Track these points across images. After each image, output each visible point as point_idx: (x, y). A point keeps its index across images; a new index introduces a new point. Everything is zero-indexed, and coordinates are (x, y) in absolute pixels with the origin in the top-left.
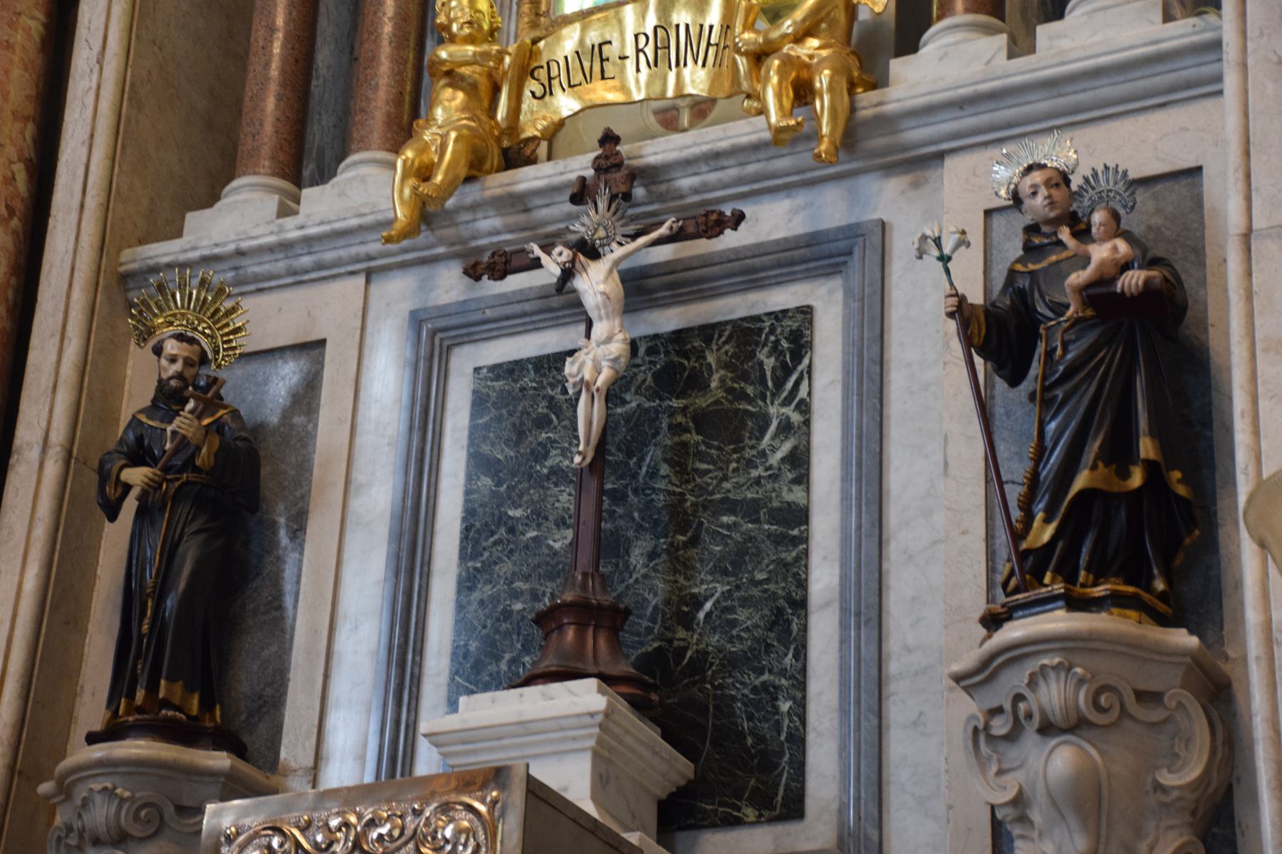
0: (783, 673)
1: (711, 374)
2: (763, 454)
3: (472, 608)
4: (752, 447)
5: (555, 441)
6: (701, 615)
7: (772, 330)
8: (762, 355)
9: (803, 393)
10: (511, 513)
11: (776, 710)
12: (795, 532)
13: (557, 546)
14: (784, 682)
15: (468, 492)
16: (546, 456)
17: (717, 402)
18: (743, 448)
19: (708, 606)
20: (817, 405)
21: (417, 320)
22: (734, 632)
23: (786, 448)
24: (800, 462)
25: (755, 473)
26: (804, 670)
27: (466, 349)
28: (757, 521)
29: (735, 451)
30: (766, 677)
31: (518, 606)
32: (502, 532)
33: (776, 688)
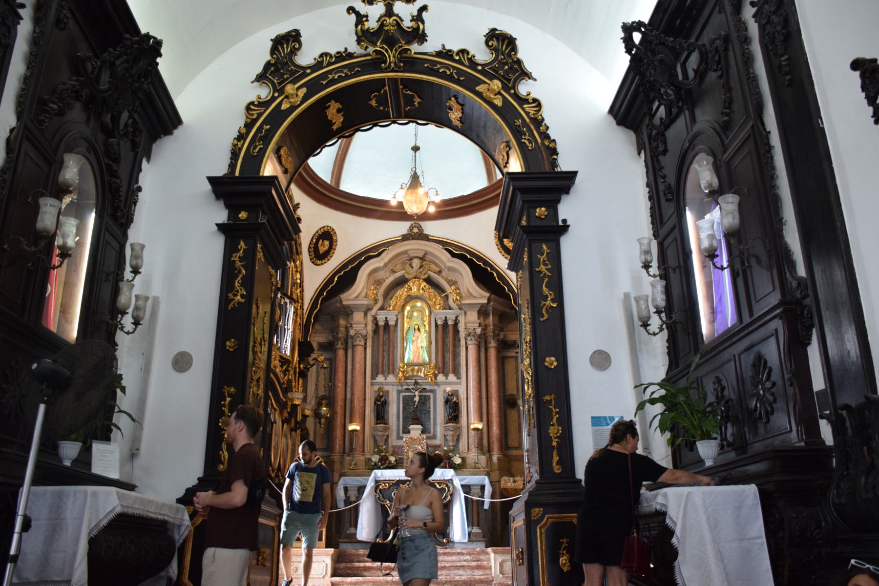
21: (398, 390)
24: (430, 407)
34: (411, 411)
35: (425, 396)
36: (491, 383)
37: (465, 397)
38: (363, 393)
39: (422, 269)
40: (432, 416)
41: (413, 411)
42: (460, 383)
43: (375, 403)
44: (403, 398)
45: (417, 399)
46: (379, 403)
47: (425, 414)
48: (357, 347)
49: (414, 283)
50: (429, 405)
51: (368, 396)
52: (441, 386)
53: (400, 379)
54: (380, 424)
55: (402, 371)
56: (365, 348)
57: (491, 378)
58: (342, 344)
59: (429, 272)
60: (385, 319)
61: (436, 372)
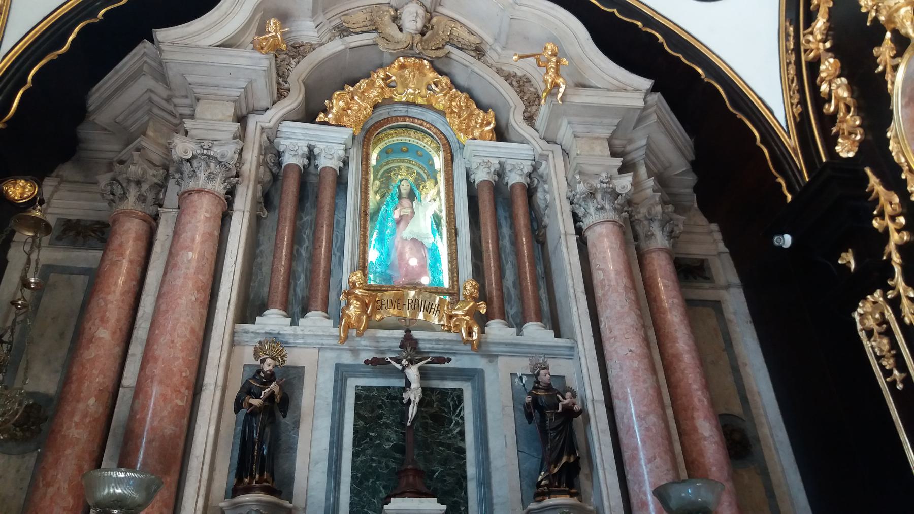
0: (461, 498)
1: (434, 403)
2: (451, 430)
3: (358, 463)
4: (448, 427)
5: (384, 414)
6: (435, 477)
7: (452, 394)
8: (449, 400)
9: (462, 414)
10: (370, 434)
11: (460, 510)
12: (462, 456)
13: (386, 447)
14: (461, 501)
15: (354, 425)
16: (382, 418)
17: (436, 412)
18: (444, 427)
19: (437, 474)
20: (465, 418)
21: (338, 367)
22: (445, 483)
23: (458, 429)
24: (462, 434)
25: (449, 435)
26: (467, 498)
27: (353, 379)
28: (450, 450)
29: (442, 428)
30: (456, 499)
31: (374, 465)
32: (368, 440)
33: (460, 502)
34: (388, 446)
35: (444, 392)
36: (677, 356)
37: (599, 395)
38: (194, 357)
39: (427, 34)
40: (471, 470)
41: (396, 448)
42: (571, 353)
43: (238, 406)
44: (358, 397)
45: (414, 395)
46: (256, 402)
47: (445, 462)
48: (195, 197)
49: (402, 67)
50: (460, 424)
51: (213, 376)
52: (501, 361)
53: (349, 326)
54: (248, 490)
55: (357, 298)
56: (225, 218)
57: (675, 341)
58: (142, 199)
59: (449, 48)
60: (306, 149)
61: (483, 310)
